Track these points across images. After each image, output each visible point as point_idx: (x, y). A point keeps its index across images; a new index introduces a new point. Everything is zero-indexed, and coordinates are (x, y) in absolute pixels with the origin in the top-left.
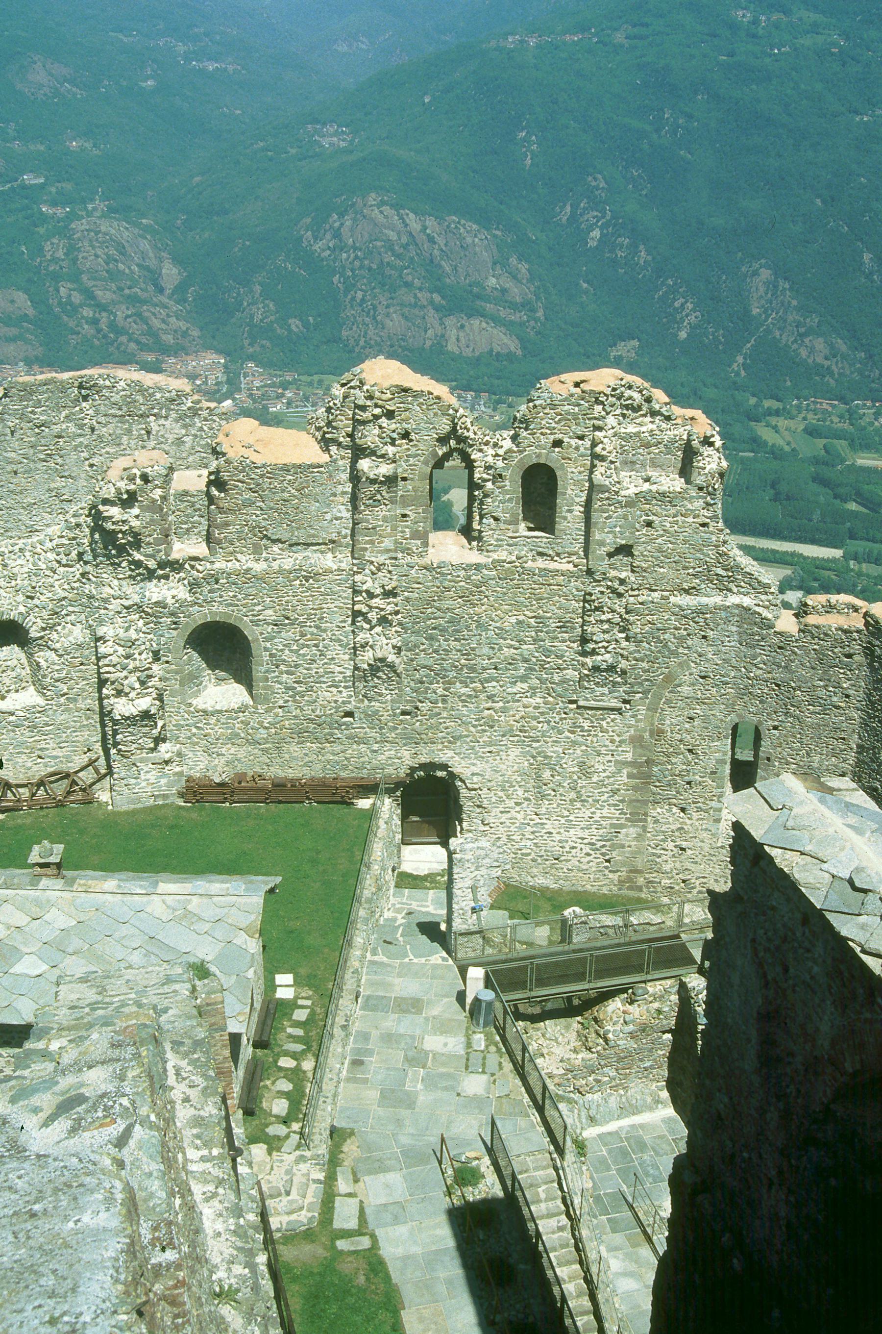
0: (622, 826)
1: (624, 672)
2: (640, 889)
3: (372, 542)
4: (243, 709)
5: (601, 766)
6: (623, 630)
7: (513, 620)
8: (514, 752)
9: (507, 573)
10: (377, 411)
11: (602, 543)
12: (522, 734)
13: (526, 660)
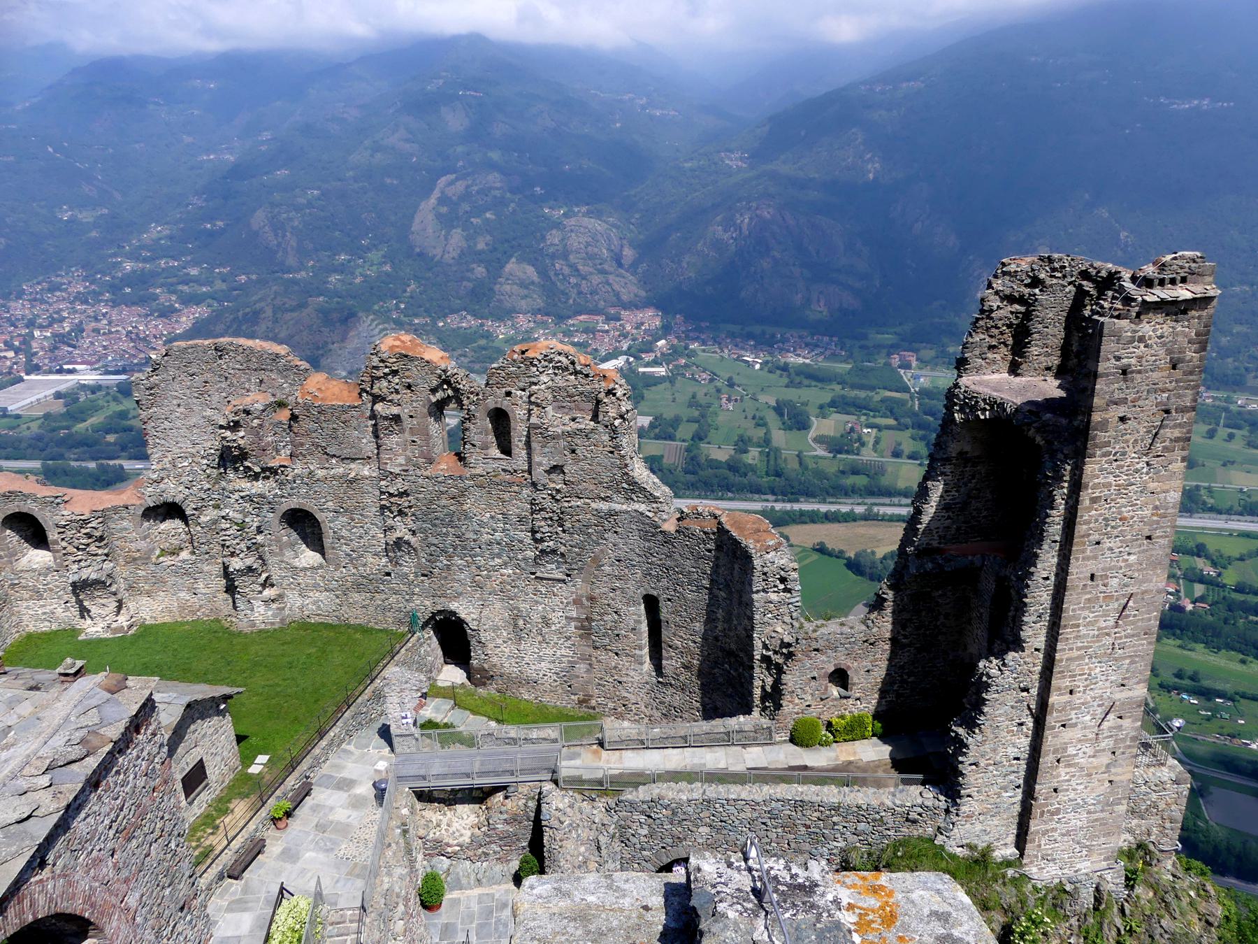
0: (576, 663)
1: (563, 555)
2: (594, 708)
3: (390, 459)
4: (321, 566)
5: (557, 617)
6: (562, 526)
7: (488, 515)
8: (498, 605)
9: (488, 483)
10: (387, 370)
11: (540, 464)
12: (503, 593)
13: (499, 544)
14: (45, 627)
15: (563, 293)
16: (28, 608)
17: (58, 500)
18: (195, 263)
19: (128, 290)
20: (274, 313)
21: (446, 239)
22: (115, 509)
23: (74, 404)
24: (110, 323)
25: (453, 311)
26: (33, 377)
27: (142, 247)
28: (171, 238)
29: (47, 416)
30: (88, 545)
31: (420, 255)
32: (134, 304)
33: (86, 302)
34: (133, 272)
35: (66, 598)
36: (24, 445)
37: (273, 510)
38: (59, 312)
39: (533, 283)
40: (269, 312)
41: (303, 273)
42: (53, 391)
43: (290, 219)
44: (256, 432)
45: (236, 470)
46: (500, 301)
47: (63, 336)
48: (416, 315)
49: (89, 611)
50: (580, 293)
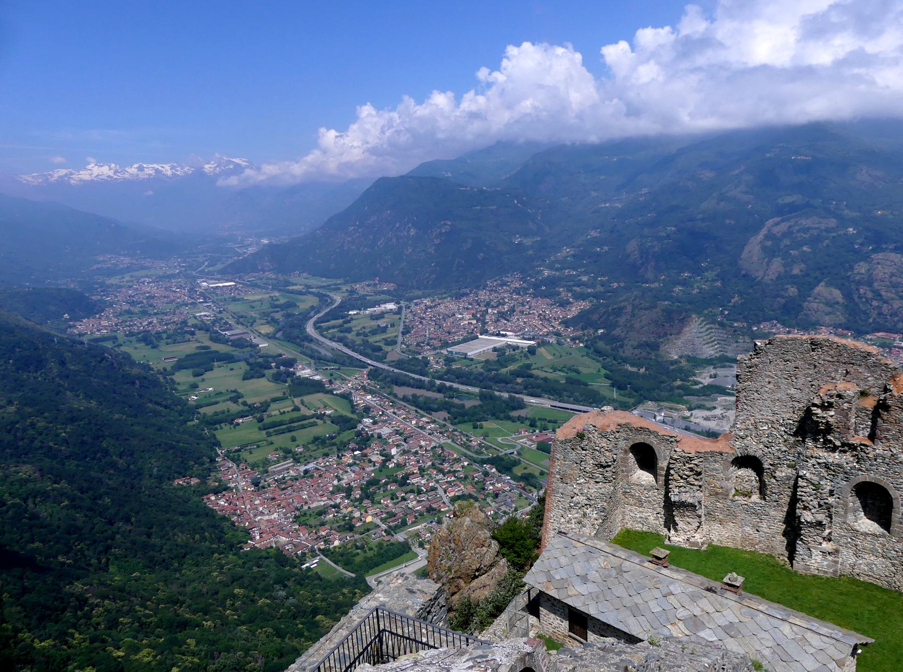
4: (884, 536)
14: (638, 527)
15: (864, 313)
16: (631, 511)
17: (672, 439)
18: (586, 273)
19: (544, 288)
20: (633, 310)
21: (768, 266)
22: (712, 454)
23: (503, 355)
24: (530, 308)
25: (766, 320)
26: (483, 337)
27: (557, 261)
28: (574, 256)
29: (487, 361)
30: (689, 476)
31: (744, 276)
32: (546, 297)
33: (519, 294)
34: (549, 276)
35: (659, 510)
36: (472, 377)
37: (847, 479)
38: (503, 298)
39: (837, 303)
40: (629, 308)
41: (656, 284)
42: (492, 346)
43: (653, 247)
44: (845, 414)
45: (816, 440)
46: (806, 315)
47: (503, 313)
48: (736, 321)
49: (675, 524)
50: (880, 314)
